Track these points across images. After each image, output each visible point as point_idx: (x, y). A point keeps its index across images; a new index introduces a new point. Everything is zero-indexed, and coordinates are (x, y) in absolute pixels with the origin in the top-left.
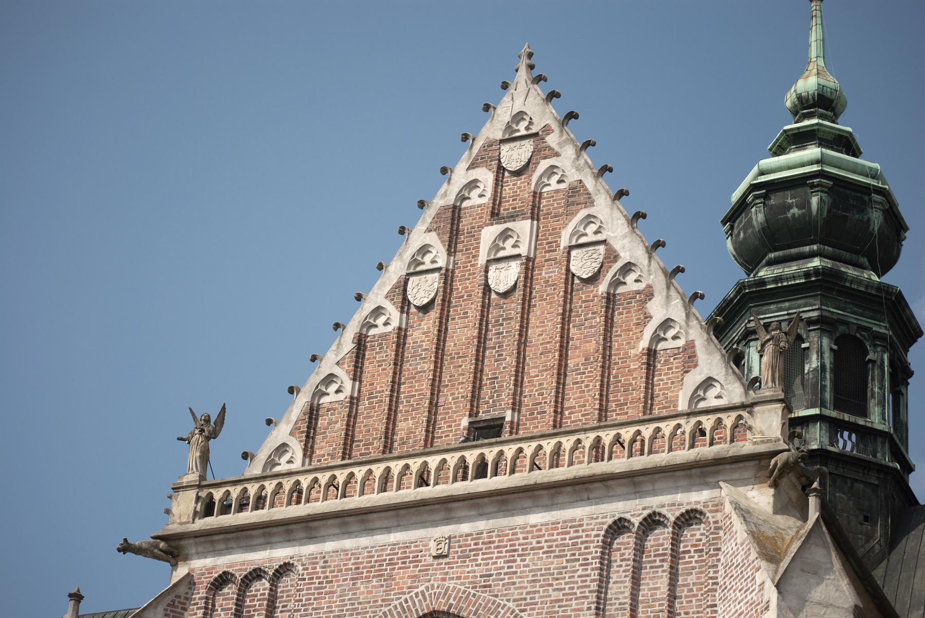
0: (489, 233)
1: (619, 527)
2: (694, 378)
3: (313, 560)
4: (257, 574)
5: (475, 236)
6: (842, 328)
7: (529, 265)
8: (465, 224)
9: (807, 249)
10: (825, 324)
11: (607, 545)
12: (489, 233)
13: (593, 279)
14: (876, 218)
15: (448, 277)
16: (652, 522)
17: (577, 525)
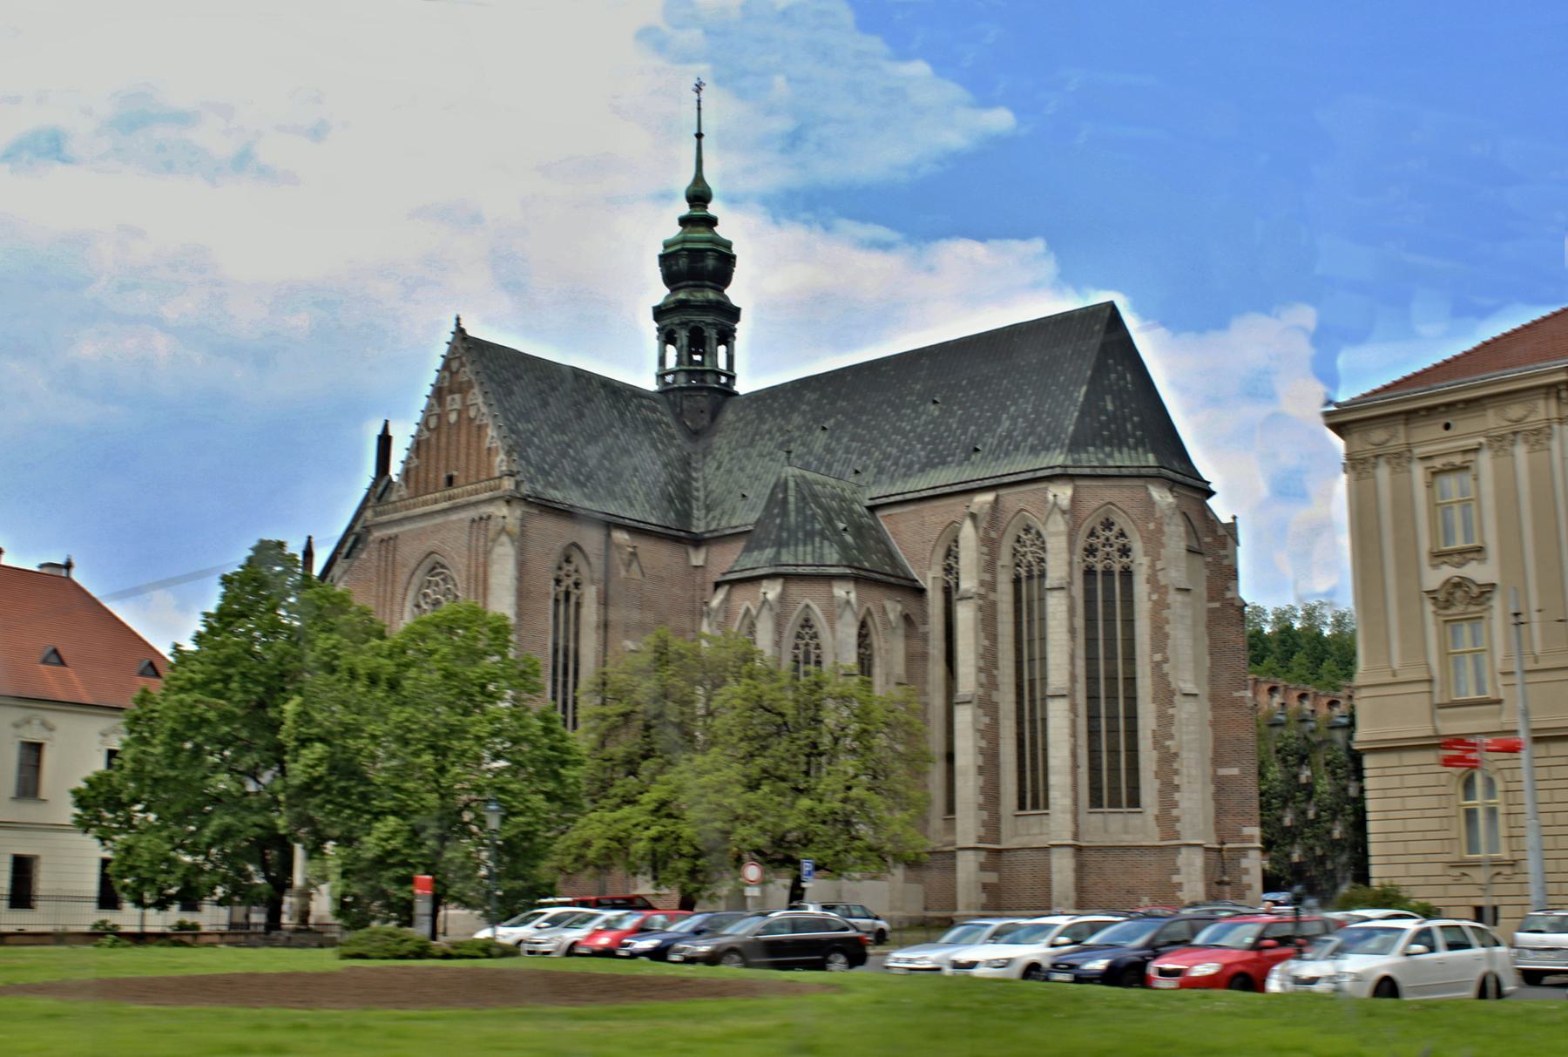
0: (449, 398)
1: (473, 521)
2: (498, 459)
3: (402, 533)
4: (390, 538)
5: (445, 399)
6: (692, 324)
7: (460, 412)
8: (445, 392)
9: (684, 283)
10: (683, 324)
11: (471, 527)
12: (449, 398)
13: (475, 419)
14: (710, 263)
15: (439, 417)
16: (481, 518)
17: (462, 520)
